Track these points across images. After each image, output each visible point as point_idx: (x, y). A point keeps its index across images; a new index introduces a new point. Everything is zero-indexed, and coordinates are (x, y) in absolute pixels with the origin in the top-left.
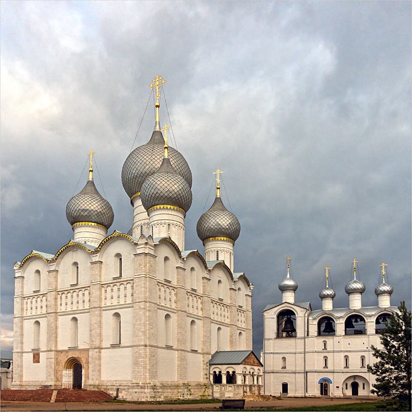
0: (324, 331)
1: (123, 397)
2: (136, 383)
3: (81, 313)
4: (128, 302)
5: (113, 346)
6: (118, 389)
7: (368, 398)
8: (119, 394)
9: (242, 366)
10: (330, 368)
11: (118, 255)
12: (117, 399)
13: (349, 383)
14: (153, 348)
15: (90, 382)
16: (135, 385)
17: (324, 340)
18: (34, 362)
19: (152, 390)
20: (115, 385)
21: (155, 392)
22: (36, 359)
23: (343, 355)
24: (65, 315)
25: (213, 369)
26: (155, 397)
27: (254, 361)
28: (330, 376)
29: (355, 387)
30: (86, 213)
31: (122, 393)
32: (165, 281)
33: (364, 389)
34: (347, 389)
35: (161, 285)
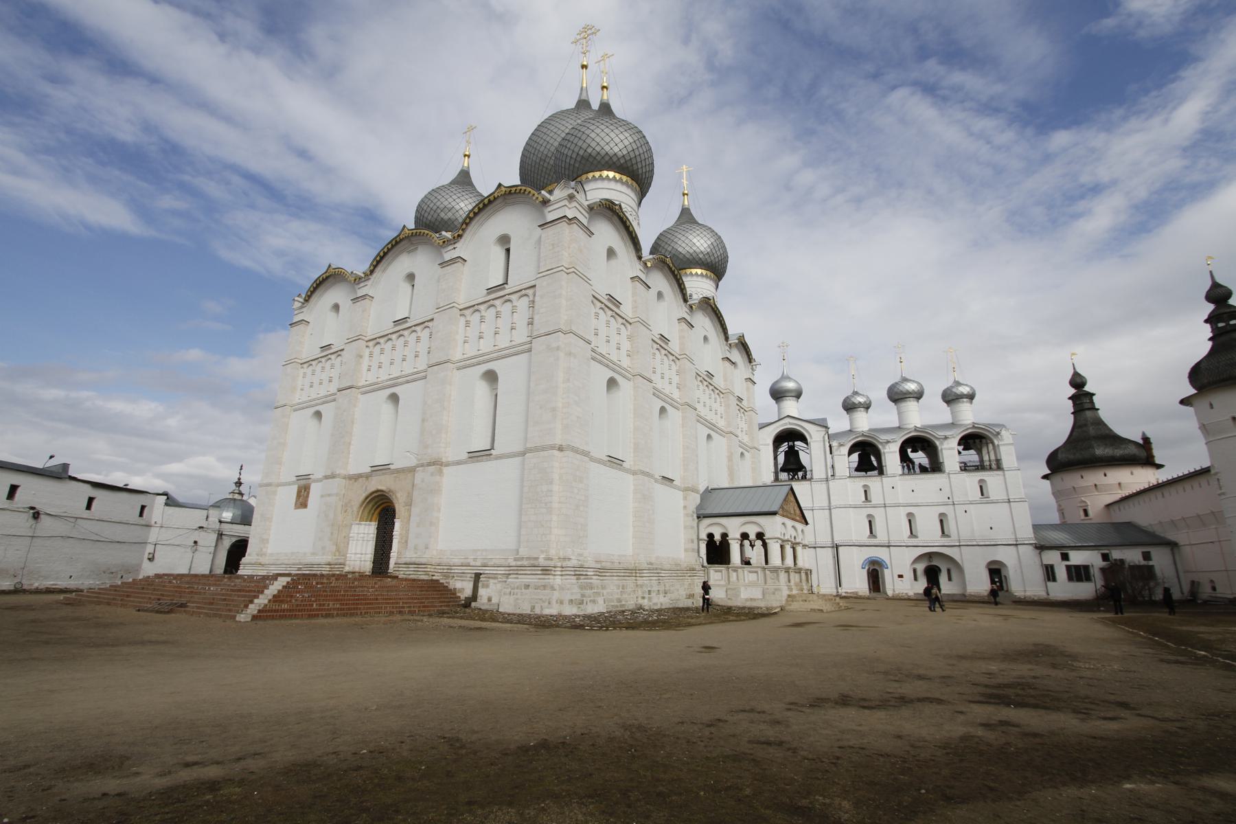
0: (857, 470)
1: (490, 600)
2: (528, 558)
3: (408, 382)
4: (518, 341)
5: (476, 456)
6: (477, 577)
7: (963, 599)
8: (482, 592)
9: (778, 518)
10: (882, 537)
11: (504, 240)
12: (473, 604)
13: (921, 567)
14: (578, 456)
15: (410, 556)
16: (525, 563)
17: (863, 484)
18: (295, 509)
19: (573, 580)
20: (472, 563)
21: (582, 587)
22: (302, 500)
23: (903, 512)
24: (374, 391)
25: (707, 527)
26: (581, 603)
27: (794, 510)
28: (881, 554)
29: (932, 574)
30: (450, 215)
31: (487, 586)
32: (609, 299)
33: (950, 579)
34: (916, 579)
35: (599, 305)
